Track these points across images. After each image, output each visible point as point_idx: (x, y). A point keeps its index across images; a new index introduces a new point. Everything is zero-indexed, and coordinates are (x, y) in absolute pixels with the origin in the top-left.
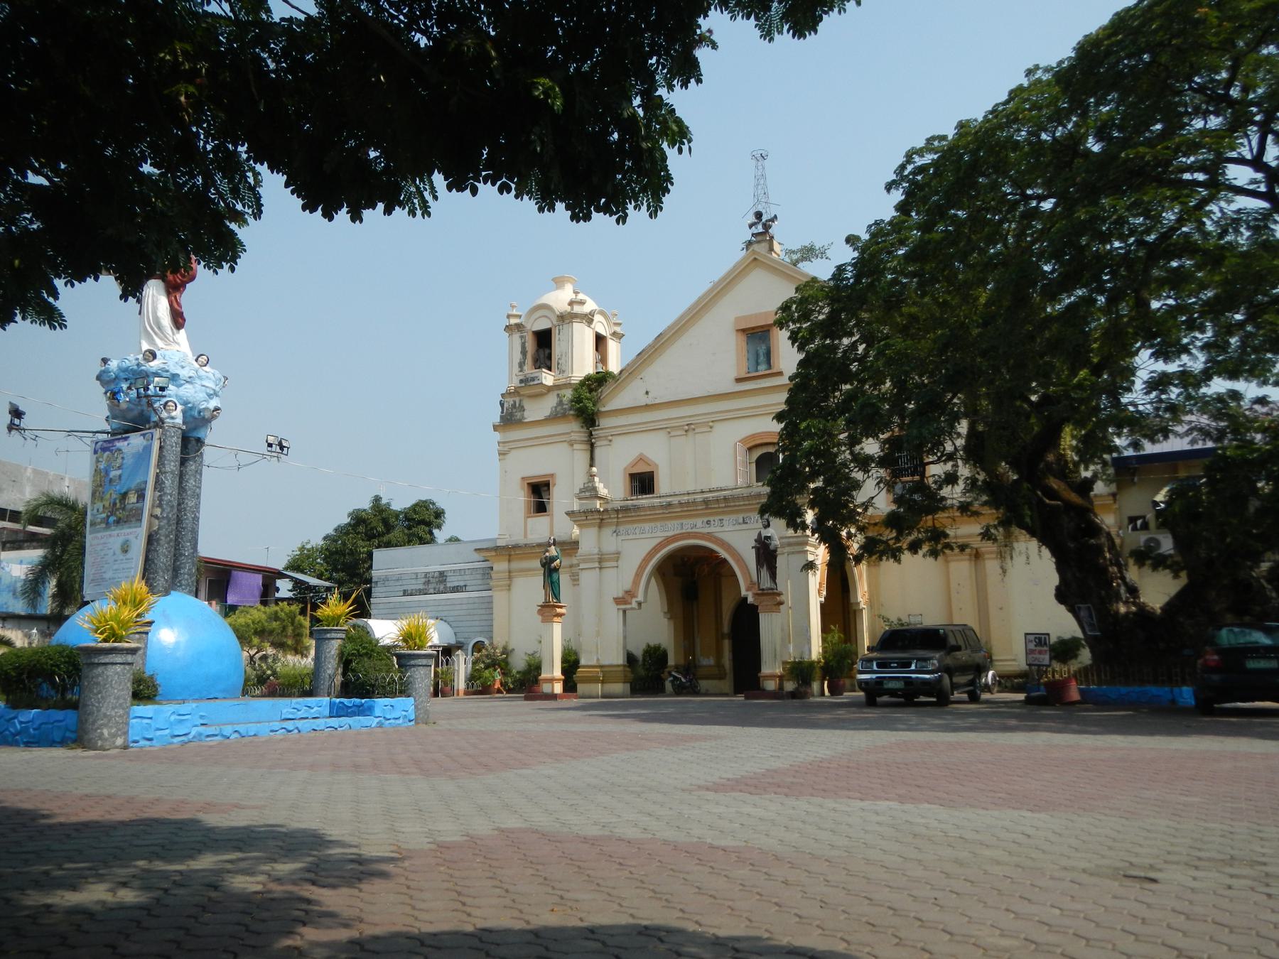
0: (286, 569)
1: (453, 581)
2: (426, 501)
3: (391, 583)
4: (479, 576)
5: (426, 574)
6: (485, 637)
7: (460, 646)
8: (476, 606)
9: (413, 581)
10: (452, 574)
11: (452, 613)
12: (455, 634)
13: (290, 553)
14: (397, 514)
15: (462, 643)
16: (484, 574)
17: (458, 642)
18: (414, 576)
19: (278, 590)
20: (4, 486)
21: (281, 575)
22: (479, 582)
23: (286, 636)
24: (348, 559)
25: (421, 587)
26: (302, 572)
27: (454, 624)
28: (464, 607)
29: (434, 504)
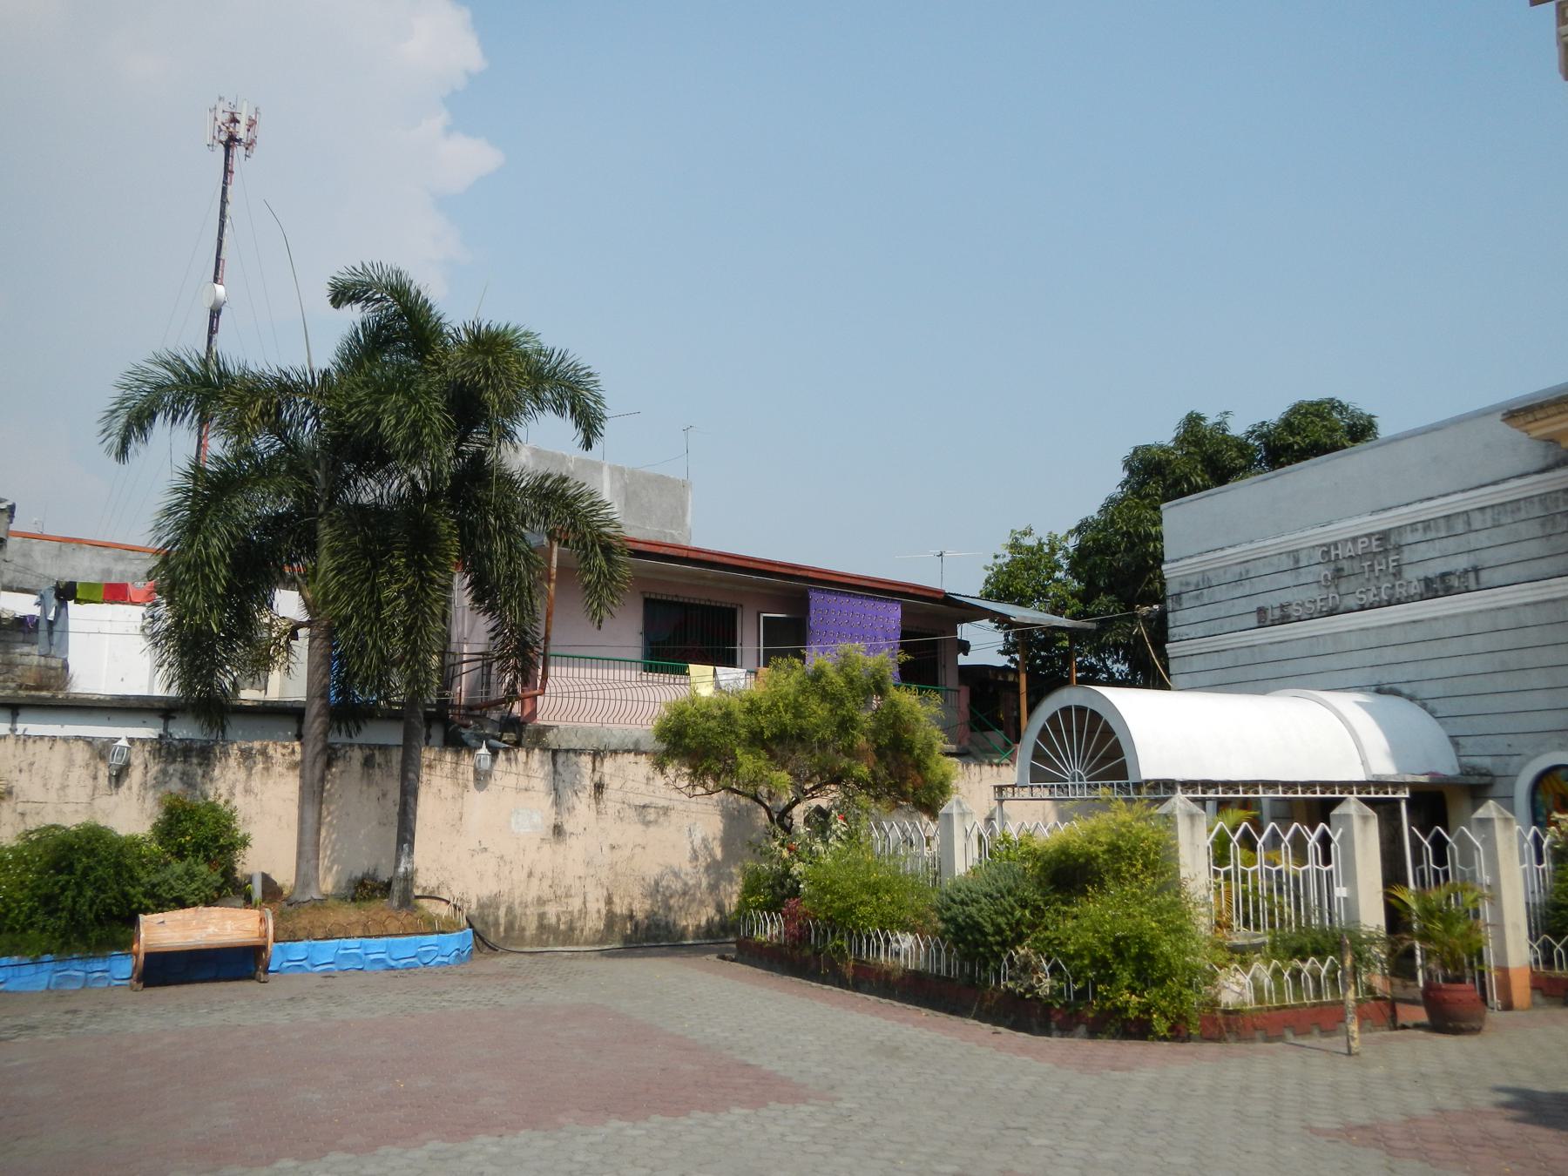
0: (987, 596)
1: (1427, 560)
2: (1319, 404)
3: (1220, 593)
4: (1534, 529)
5: (1327, 551)
7: (1477, 787)
8: (1532, 636)
9: (1287, 579)
10: (1418, 536)
11: (1435, 669)
13: (990, 562)
14: (1241, 446)
15: (1488, 774)
16: (1547, 519)
17: (1468, 771)
18: (1288, 563)
19: (964, 647)
21: (972, 613)
22: (1534, 548)
23: (850, 751)
24: (1121, 559)
25: (1315, 593)
26: (1023, 601)
27: (1443, 708)
28: (1478, 643)
29: (1342, 408)
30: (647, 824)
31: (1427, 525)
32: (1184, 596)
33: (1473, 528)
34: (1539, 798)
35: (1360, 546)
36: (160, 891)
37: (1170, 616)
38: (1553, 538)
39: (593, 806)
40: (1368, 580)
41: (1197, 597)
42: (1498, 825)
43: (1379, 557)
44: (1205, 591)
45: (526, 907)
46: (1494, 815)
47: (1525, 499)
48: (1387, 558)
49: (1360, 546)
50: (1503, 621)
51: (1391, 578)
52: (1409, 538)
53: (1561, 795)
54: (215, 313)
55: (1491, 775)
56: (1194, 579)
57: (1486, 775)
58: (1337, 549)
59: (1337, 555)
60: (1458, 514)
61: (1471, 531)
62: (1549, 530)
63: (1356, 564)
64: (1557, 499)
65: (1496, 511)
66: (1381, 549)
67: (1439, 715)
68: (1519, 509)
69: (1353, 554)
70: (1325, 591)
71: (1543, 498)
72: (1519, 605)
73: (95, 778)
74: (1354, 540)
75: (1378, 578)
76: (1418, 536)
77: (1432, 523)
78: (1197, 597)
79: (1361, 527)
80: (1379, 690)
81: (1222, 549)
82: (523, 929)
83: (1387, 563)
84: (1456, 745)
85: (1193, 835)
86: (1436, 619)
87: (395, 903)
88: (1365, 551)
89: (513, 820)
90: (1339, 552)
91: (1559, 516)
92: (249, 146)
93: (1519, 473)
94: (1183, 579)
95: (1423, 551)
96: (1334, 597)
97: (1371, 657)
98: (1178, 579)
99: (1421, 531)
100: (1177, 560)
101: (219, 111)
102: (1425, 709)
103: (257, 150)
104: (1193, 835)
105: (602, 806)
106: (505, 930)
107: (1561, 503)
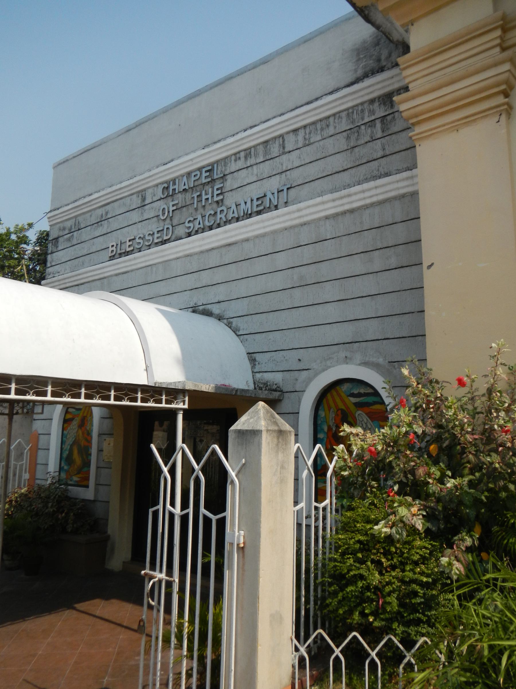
3: (85, 234)
4: (341, 143)
6: (365, 364)
9: (135, 216)
10: (240, 164)
12: (252, 357)
18: (136, 201)
31: (248, 153)
32: (61, 240)
33: (287, 150)
34: (322, 413)
35: (193, 179)
37: (49, 257)
38: (356, 150)
40: (196, 209)
41: (69, 240)
42: (266, 439)
43: (207, 188)
44: (75, 233)
46: (262, 424)
47: (334, 115)
48: (213, 188)
49: (193, 179)
50: (305, 237)
51: (215, 206)
52: (233, 166)
53: (342, 410)
55: (281, 391)
56: (68, 224)
57: (275, 390)
58: (174, 184)
59: (174, 190)
60: (275, 138)
61: (284, 153)
62: (352, 144)
63: (188, 195)
64: (363, 111)
65: (308, 131)
66: (209, 179)
67: (241, 333)
68: (328, 126)
69: (186, 187)
70: (162, 224)
71: (350, 112)
72: (320, 219)
74: (189, 174)
75: (204, 206)
76: (240, 164)
77: (253, 150)
78: (69, 240)
79: (194, 161)
80: (195, 310)
81: (90, 195)
83: (213, 192)
84: (253, 361)
86: (247, 240)
88: (196, 183)
90: (176, 187)
91: (363, 127)
93: (331, 90)
94: (61, 225)
95: (244, 177)
96: (168, 228)
97: (190, 281)
98: (58, 226)
99: (243, 159)
100: (58, 209)
102: (230, 327)
107: (367, 114)
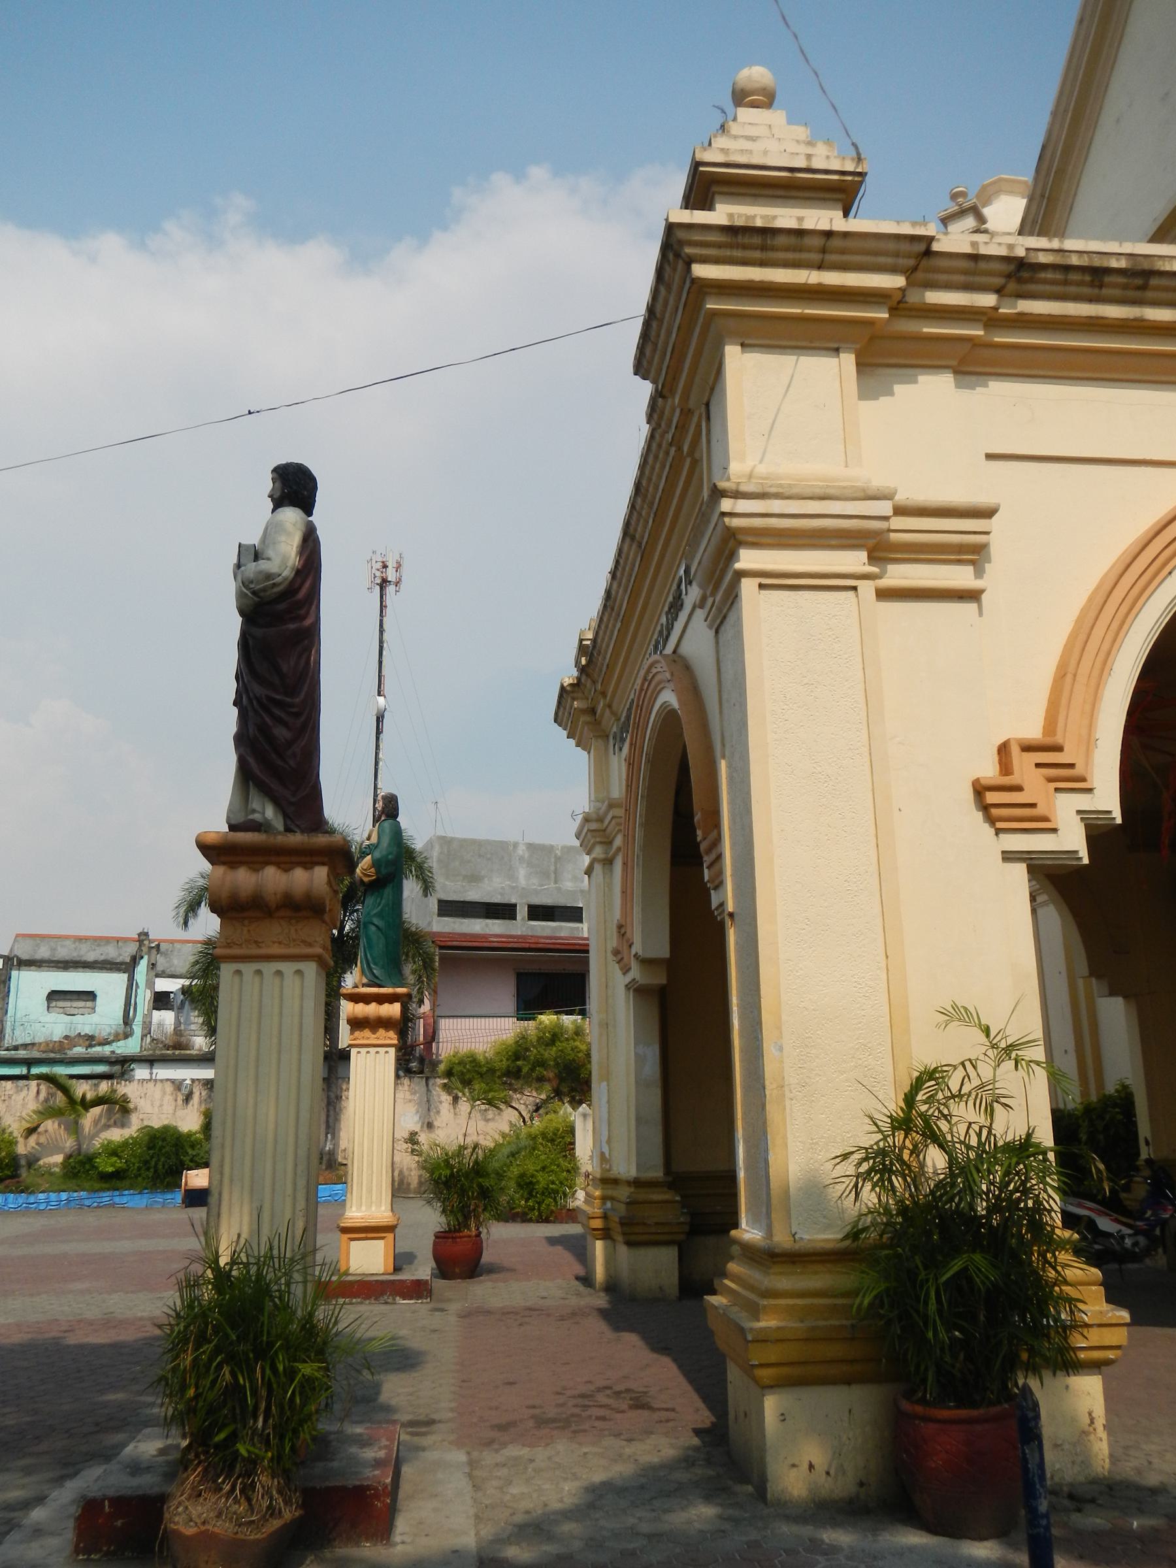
20: (483, 873)
30: (487, 1120)
36: (196, 1159)
39: (452, 1110)
45: (411, 1170)
54: (380, 719)
73: (176, 1100)
82: (409, 1184)
85: (585, 1125)
87: (324, 1167)
89: (402, 1119)
92: (397, 584)
101: (374, 562)
103: (403, 586)
104: (585, 1125)
105: (457, 1110)
106: (398, 1184)
